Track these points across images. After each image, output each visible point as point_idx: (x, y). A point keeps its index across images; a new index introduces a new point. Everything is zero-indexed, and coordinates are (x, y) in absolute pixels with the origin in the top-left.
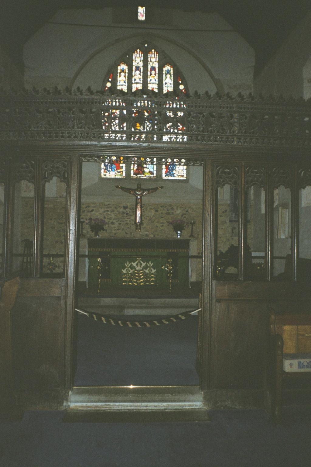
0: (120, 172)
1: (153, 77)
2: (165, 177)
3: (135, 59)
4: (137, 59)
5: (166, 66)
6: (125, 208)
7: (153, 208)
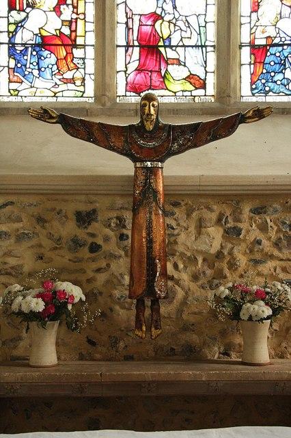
0: (72, 81)
6: (85, 218)
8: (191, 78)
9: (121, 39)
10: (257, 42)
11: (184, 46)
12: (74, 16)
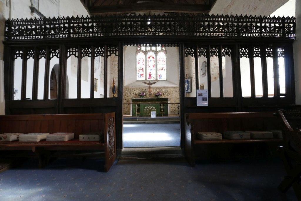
6: (145, 89)
8: (154, 78)
9: (147, 74)
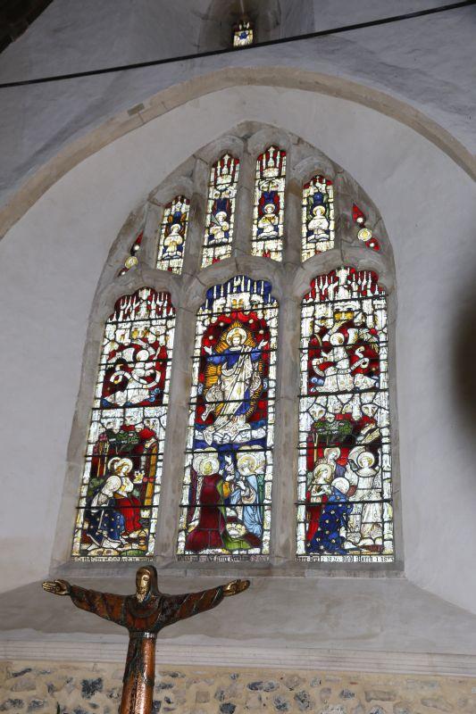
0: (136, 540)
1: (270, 219)
2: (307, 554)
3: (216, 180)
4: (220, 180)
5: (312, 183)
7: (212, 690)
10: (314, 500)
11: (243, 505)
12: (146, 480)
